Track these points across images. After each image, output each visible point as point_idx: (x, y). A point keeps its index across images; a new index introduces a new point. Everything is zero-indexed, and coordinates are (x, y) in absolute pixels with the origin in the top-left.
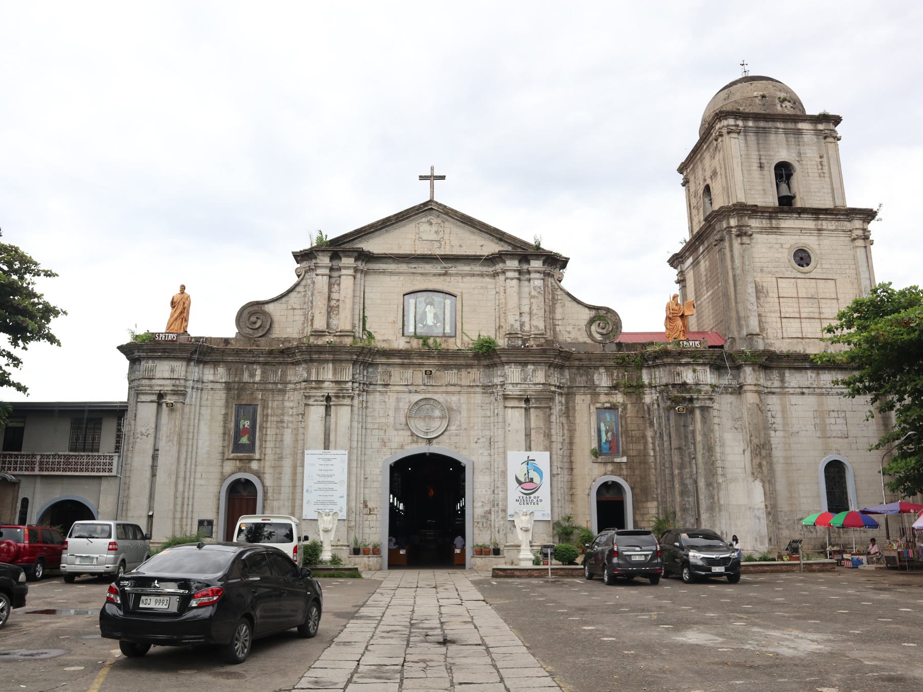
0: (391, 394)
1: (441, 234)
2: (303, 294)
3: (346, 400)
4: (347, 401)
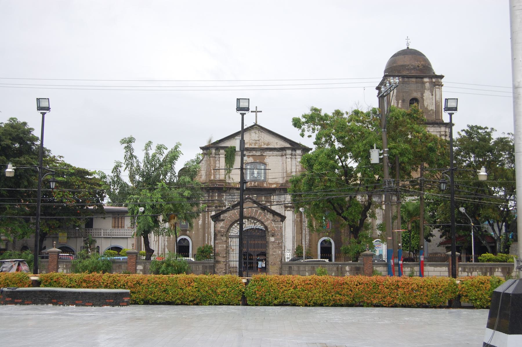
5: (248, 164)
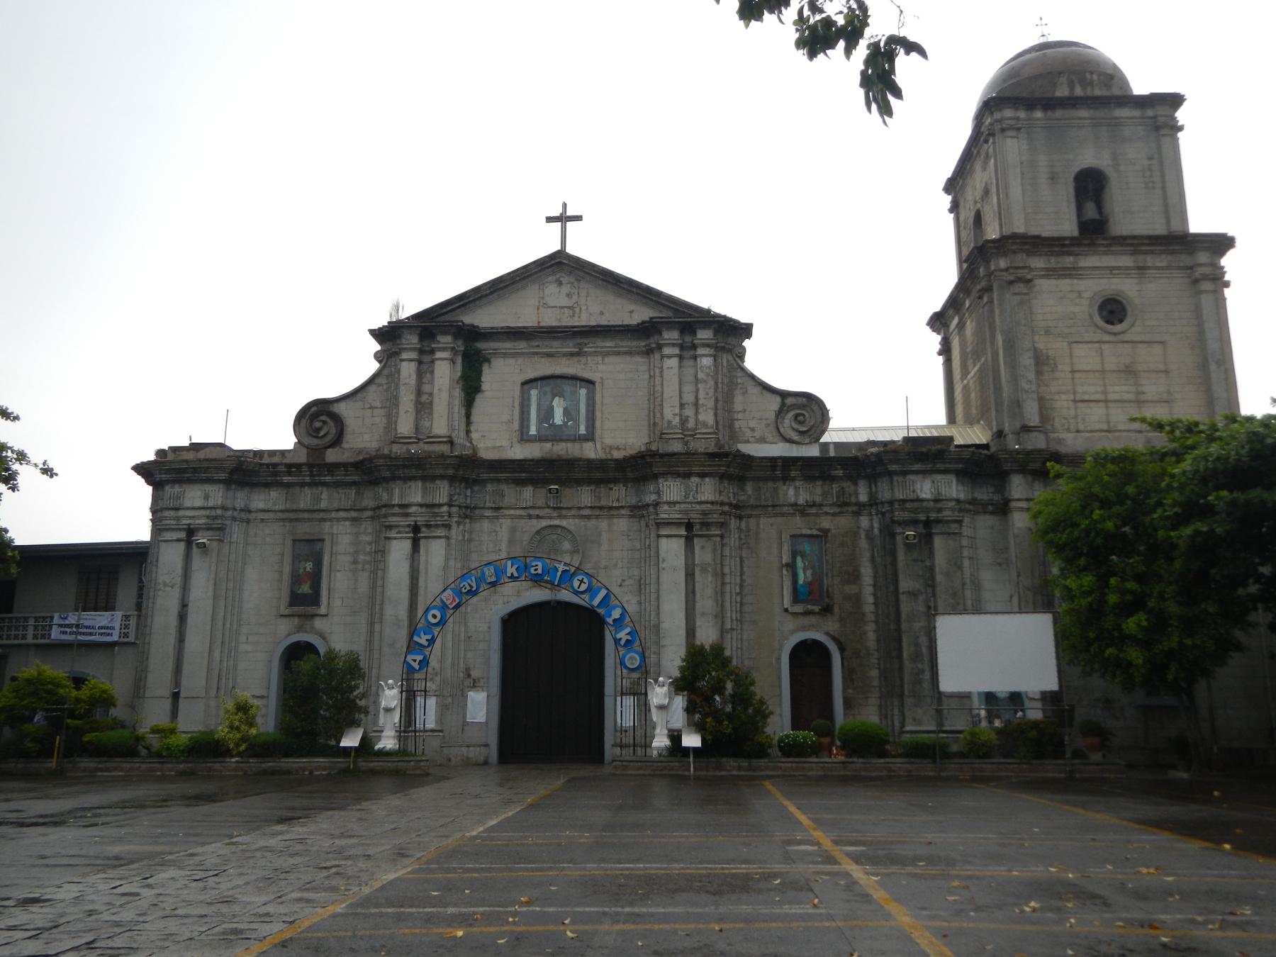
0: (504, 520)
1: (575, 297)
2: (385, 387)
3: (439, 531)
4: (440, 532)
5: (534, 384)
